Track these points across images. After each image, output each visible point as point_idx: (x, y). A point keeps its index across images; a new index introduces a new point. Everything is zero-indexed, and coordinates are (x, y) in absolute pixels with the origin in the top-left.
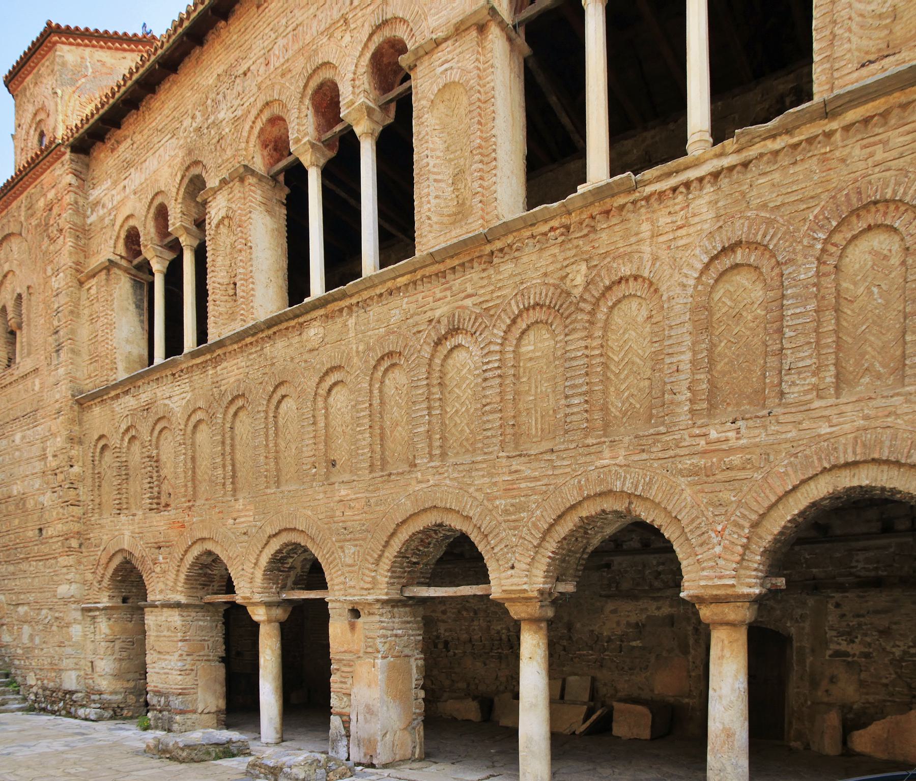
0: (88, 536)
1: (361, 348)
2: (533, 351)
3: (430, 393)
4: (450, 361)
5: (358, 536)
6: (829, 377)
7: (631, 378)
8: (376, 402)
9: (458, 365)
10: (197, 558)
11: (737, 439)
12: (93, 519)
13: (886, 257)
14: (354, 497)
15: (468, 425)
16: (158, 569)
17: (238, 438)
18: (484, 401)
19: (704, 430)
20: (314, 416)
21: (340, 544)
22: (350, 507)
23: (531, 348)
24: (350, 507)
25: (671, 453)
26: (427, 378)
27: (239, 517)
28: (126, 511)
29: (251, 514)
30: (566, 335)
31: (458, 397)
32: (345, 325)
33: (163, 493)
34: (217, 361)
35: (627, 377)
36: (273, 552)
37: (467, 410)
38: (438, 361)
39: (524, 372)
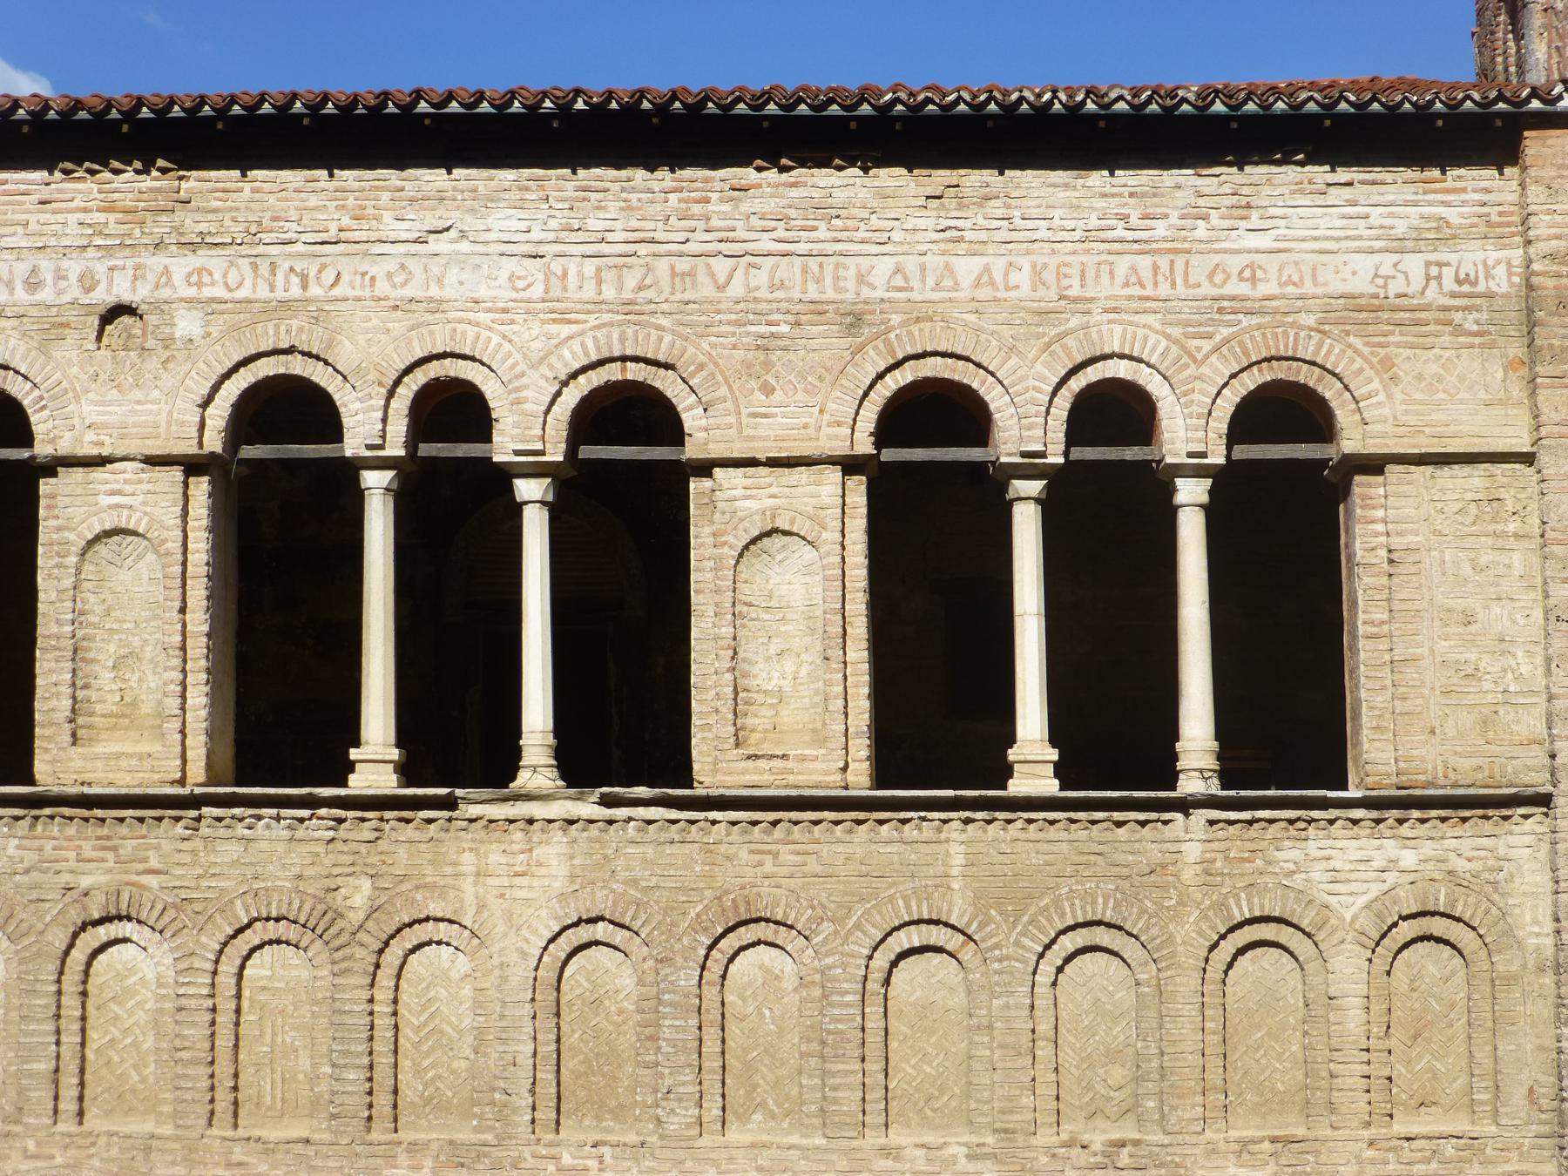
2: (270, 978)
6: (713, 1109)
7: (439, 1053)
15: (135, 1067)
18: (178, 1043)
19: (554, 1151)
31: (116, 1018)
35: (432, 1050)
38: (78, 956)
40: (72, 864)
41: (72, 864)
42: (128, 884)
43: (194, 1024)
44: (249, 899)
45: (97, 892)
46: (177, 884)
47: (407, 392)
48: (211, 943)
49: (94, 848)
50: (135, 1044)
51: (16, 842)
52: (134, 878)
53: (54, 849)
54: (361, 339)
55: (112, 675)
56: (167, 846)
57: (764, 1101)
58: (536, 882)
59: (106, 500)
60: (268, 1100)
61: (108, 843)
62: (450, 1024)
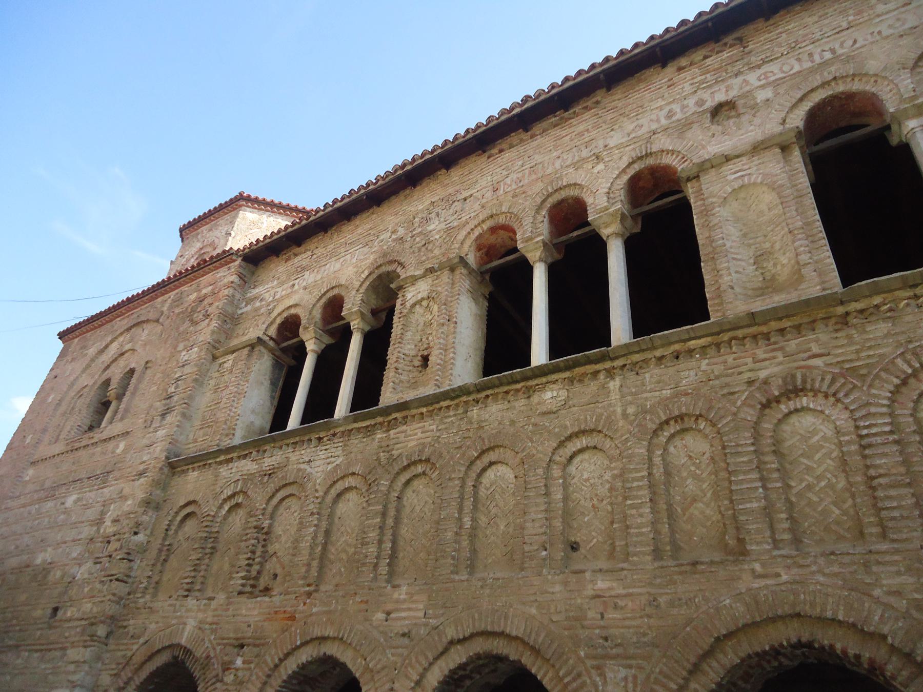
0: (125, 624)
1: (631, 410)
4: (786, 428)
5: (632, 651)
8: (658, 472)
10: (303, 667)
12: (141, 600)
15: (835, 504)
16: (229, 678)
17: (407, 510)
20: (546, 486)
21: (595, 663)
22: (616, 607)
24: (616, 607)
27: (397, 610)
28: (197, 594)
29: (421, 606)
31: (809, 469)
32: (603, 387)
33: (265, 573)
34: (391, 425)
36: (452, 666)
40: (751, 365)
41: (751, 365)
42: (797, 368)
43: (885, 455)
44: (909, 356)
45: (774, 379)
46: (839, 359)
48: (881, 392)
49: (765, 352)
50: (830, 486)
51: (707, 361)
52: (803, 363)
53: (735, 359)
55: (754, 267)
56: (823, 337)
61: (777, 346)
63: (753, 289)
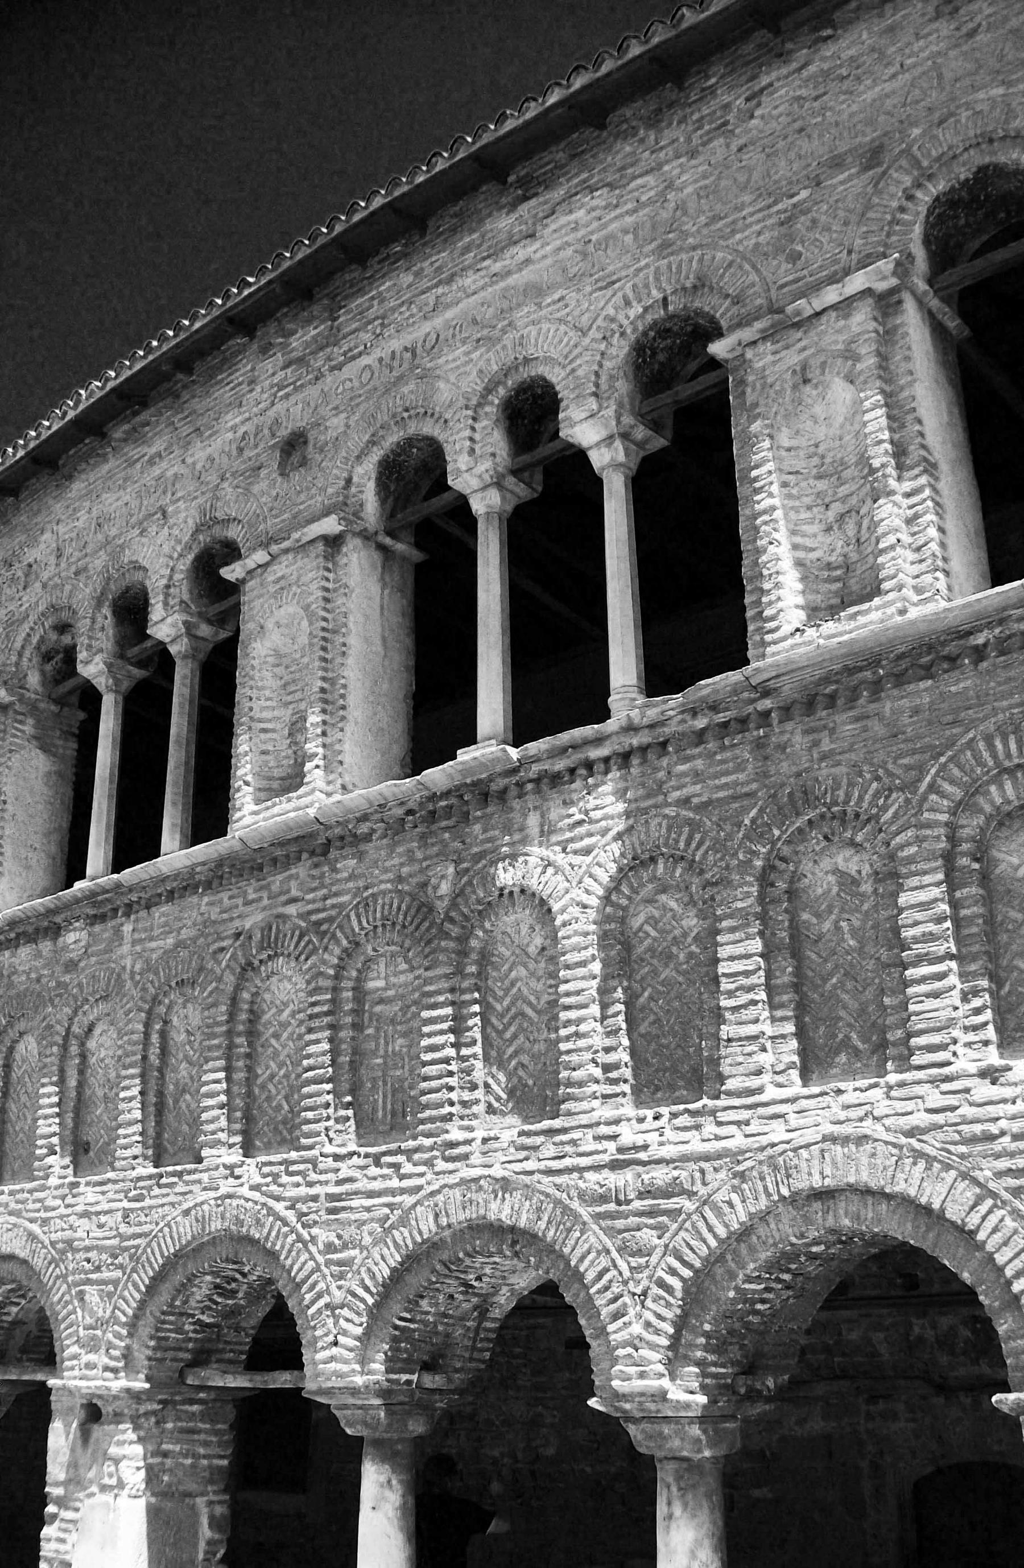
1: (138, 967)
2: (385, 989)
3: (231, 1046)
7: (521, 1038)
8: (154, 1051)
9: (278, 1002)
11: (661, 1144)
13: (855, 882)
14: (106, 1207)
23: (380, 984)
25: (567, 1162)
26: (228, 1022)
30: (427, 969)
35: (515, 1036)
37: (286, 1076)
39: (371, 1020)
46: (310, 907)
47: (491, 410)
52: (281, 910)
54: (452, 379)
57: (848, 1037)
58: (594, 828)
59: (272, 589)
60: (380, 1114)
62: (530, 1004)
63: (282, 779)
